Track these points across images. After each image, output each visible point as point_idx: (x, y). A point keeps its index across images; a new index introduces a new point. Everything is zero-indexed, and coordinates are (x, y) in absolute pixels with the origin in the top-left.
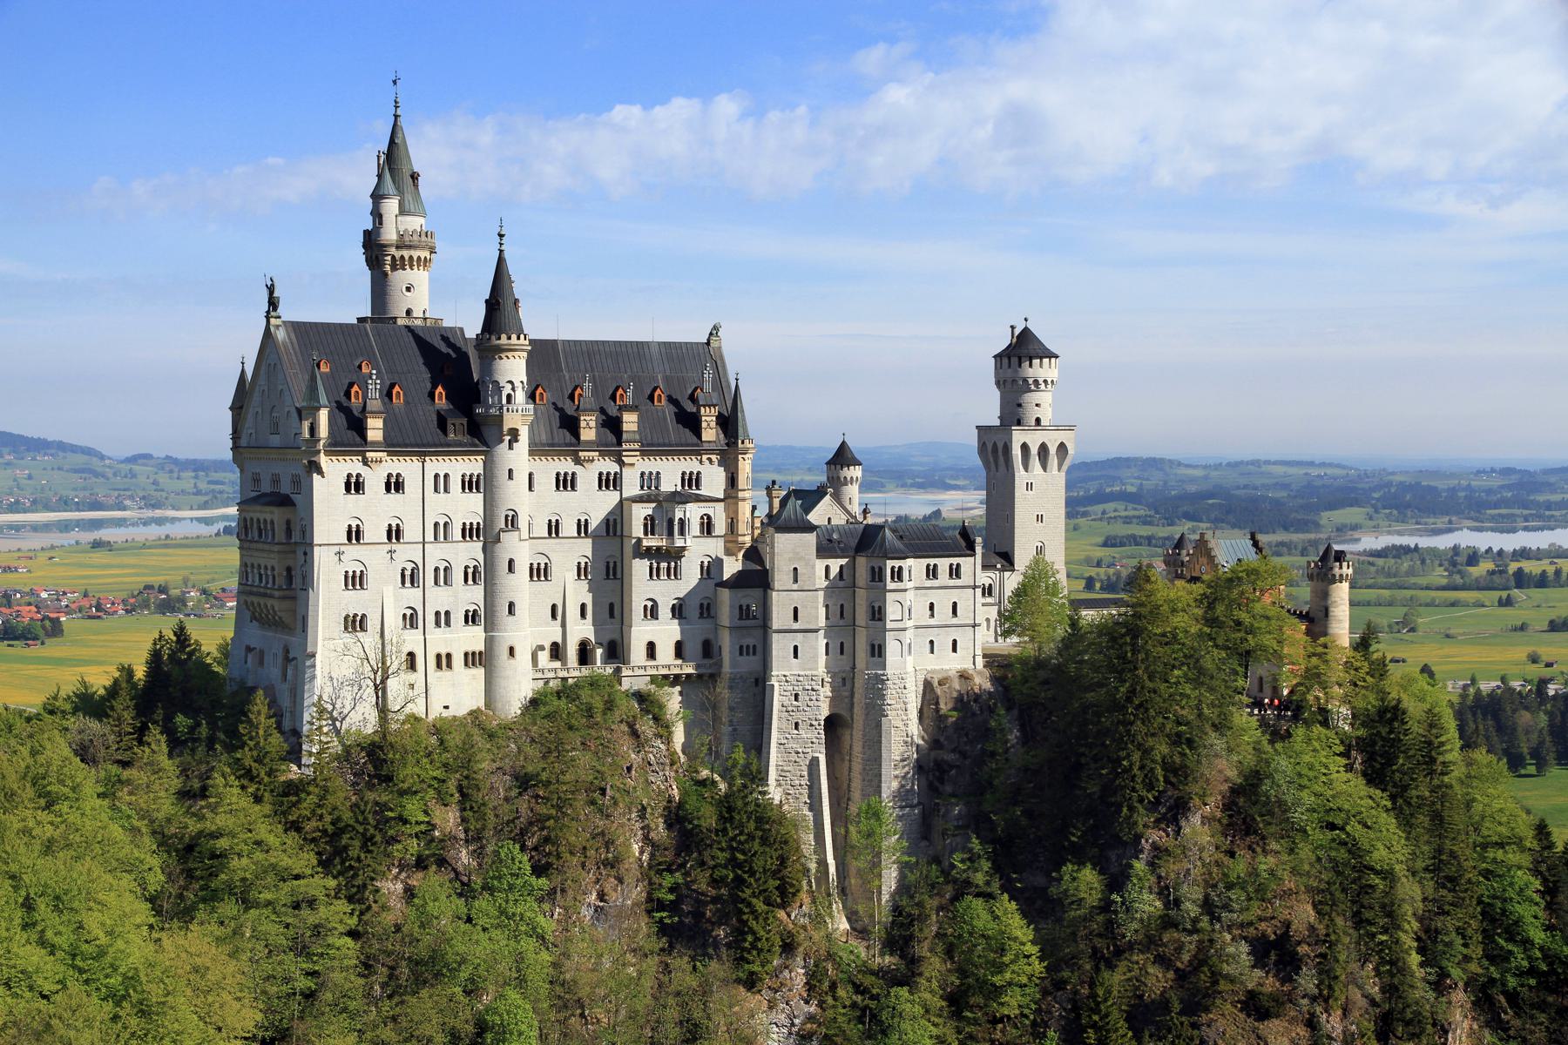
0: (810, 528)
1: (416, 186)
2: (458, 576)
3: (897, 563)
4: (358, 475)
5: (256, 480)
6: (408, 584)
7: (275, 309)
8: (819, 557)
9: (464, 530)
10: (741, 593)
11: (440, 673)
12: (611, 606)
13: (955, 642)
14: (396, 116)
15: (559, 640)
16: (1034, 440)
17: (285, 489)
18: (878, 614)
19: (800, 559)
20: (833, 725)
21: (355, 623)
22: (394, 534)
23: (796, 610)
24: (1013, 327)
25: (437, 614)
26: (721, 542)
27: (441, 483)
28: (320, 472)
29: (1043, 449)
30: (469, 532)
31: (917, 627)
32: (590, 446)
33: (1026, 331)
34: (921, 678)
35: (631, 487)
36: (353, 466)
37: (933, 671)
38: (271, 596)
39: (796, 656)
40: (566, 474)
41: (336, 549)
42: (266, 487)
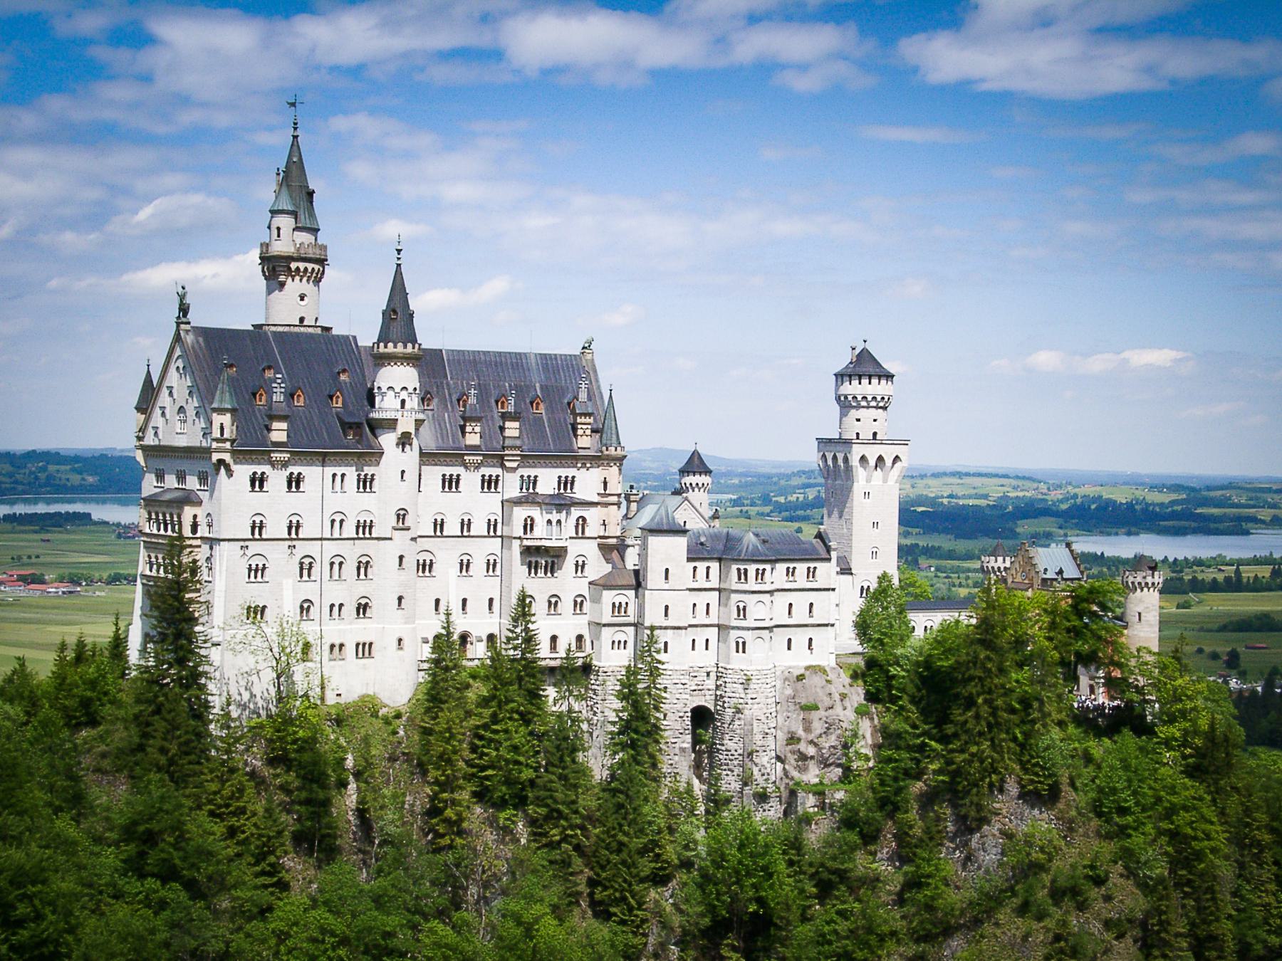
0: (682, 531)
1: (311, 202)
2: (350, 568)
3: (761, 567)
4: (263, 473)
6: (305, 577)
7: (185, 316)
8: (689, 560)
9: (358, 527)
12: (491, 600)
14: (295, 137)
16: (872, 453)
18: (742, 612)
20: (701, 717)
21: (256, 612)
22: (294, 527)
23: (667, 607)
25: (332, 606)
26: (594, 544)
28: (230, 473)
29: (880, 459)
30: (364, 528)
33: (865, 351)
40: (451, 475)
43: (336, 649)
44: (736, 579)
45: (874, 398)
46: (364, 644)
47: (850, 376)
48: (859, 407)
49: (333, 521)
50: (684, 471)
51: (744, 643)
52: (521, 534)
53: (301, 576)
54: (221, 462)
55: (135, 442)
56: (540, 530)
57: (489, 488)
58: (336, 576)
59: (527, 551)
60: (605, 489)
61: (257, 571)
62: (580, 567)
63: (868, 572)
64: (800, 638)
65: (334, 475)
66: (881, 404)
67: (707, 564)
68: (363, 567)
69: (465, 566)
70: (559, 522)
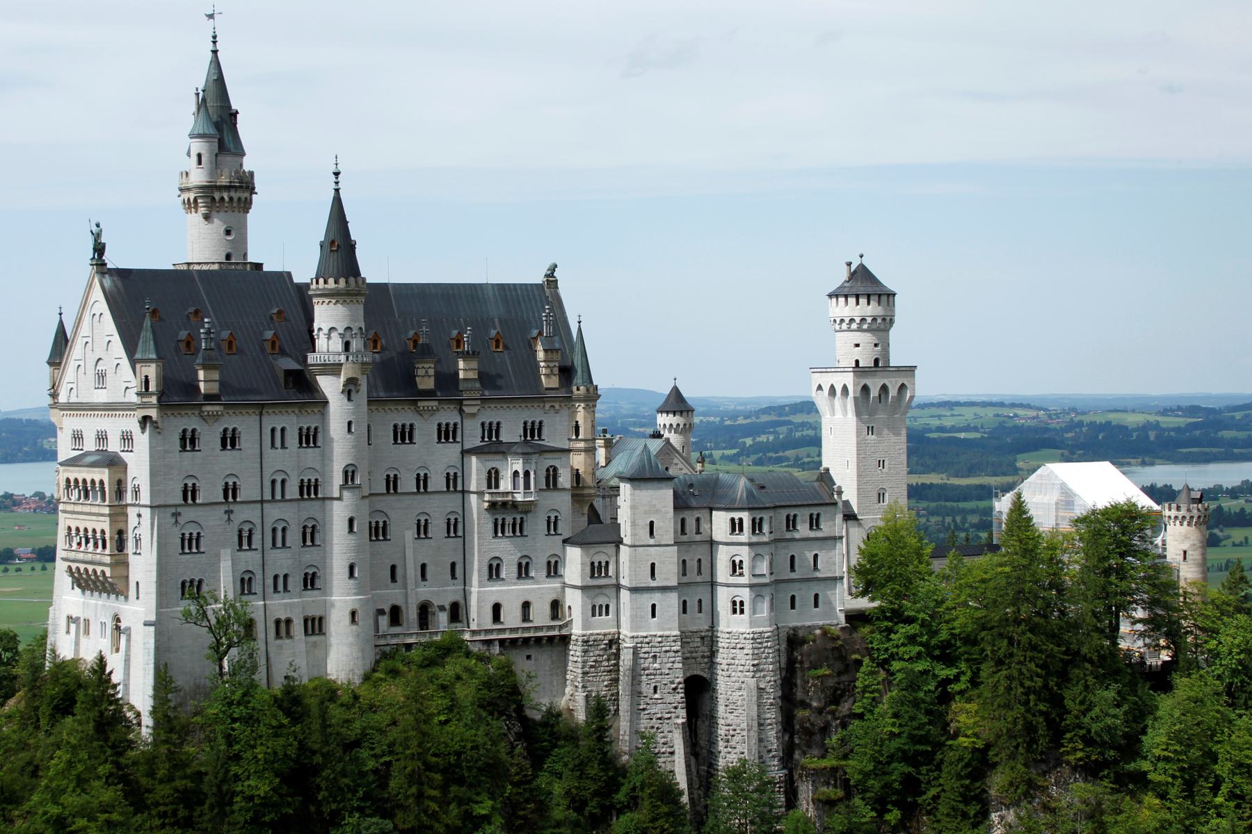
2: (294, 537)
4: (194, 431)
5: (78, 437)
6: (245, 547)
9: (301, 488)
10: (592, 551)
11: (279, 642)
12: (453, 565)
13: (816, 596)
14: (215, 52)
15: (398, 603)
17: (114, 446)
19: (657, 511)
21: (193, 589)
22: (230, 491)
23: (653, 565)
24: (849, 264)
25: (276, 577)
27: (278, 438)
29: (884, 388)
31: (777, 582)
32: (428, 394)
34: (783, 636)
35: (473, 440)
36: (191, 422)
37: (795, 629)
38: (100, 564)
39: (653, 615)
41: (173, 510)
42: (90, 445)
43: (283, 625)
44: (729, 529)
45: (874, 319)
46: (313, 620)
47: (846, 297)
48: (859, 330)
49: (273, 482)
50: (660, 411)
51: (742, 603)
52: (484, 487)
53: (240, 544)
54: (145, 420)
55: (50, 401)
56: (505, 485)
57: (447, 438)
58: (279, 544)
59: (493, 505)
60: (577, 434)
61: (191, 543)
62: (552, 525)
63: (873, 518)
64: (805, 595)
65: (273, 430)
66: (882, 327)
67: (697, 514)
68: (311, 535)
69: (422, 529)
70: (527, 474)
